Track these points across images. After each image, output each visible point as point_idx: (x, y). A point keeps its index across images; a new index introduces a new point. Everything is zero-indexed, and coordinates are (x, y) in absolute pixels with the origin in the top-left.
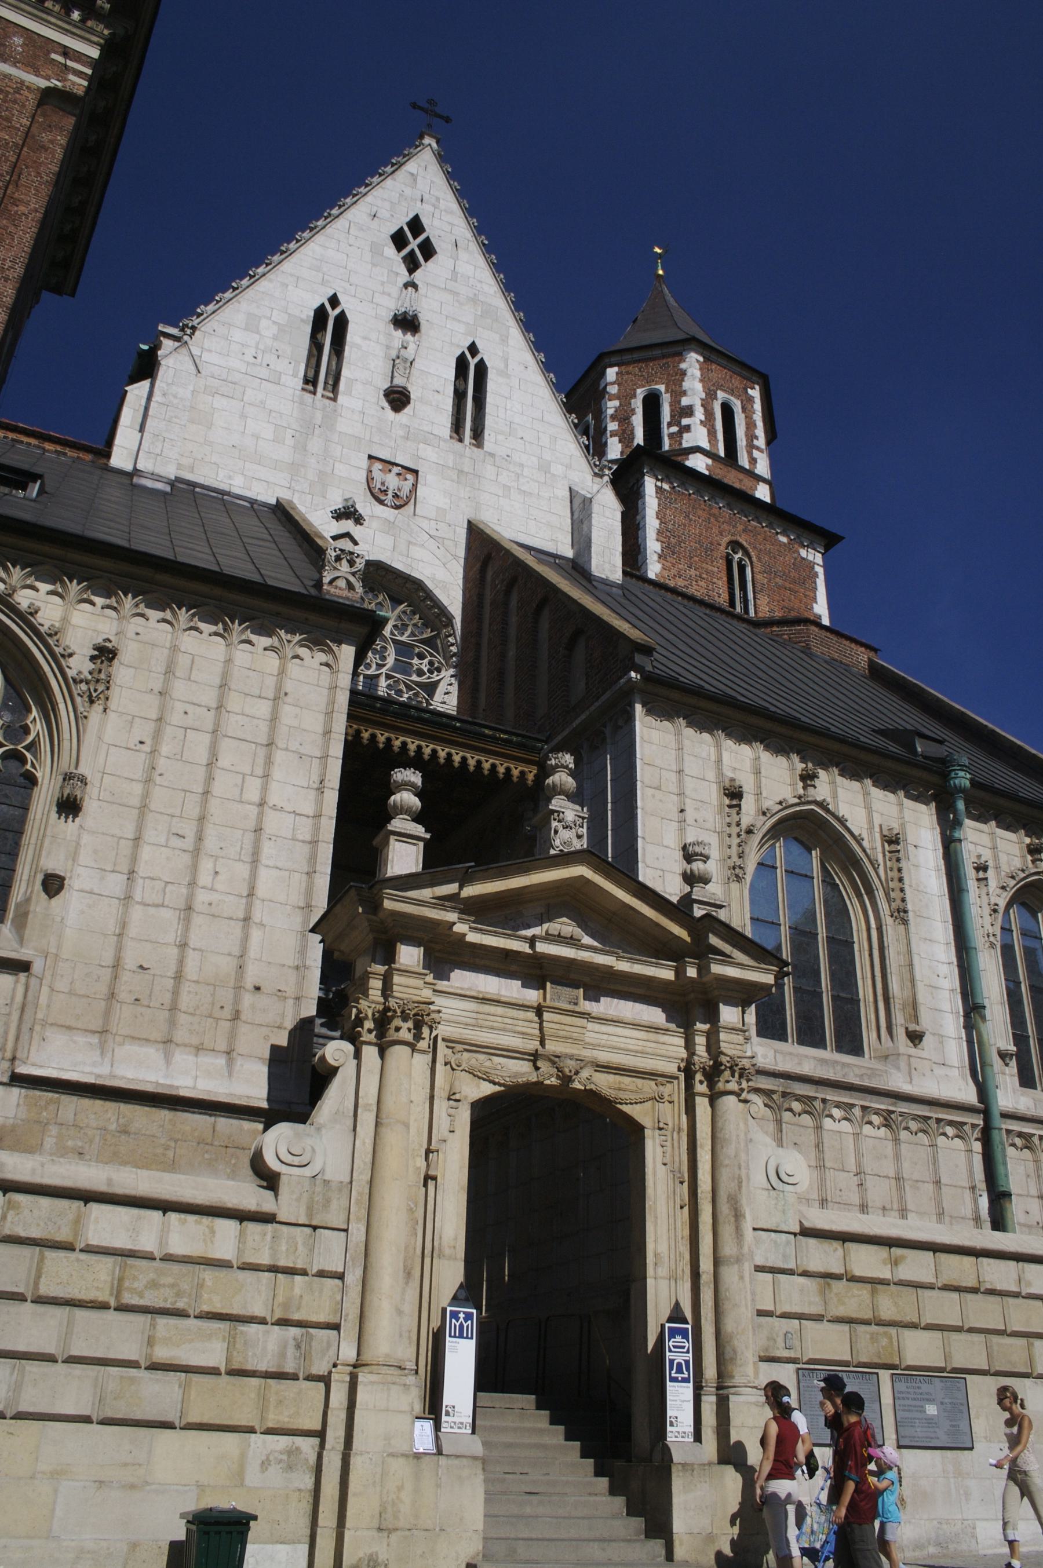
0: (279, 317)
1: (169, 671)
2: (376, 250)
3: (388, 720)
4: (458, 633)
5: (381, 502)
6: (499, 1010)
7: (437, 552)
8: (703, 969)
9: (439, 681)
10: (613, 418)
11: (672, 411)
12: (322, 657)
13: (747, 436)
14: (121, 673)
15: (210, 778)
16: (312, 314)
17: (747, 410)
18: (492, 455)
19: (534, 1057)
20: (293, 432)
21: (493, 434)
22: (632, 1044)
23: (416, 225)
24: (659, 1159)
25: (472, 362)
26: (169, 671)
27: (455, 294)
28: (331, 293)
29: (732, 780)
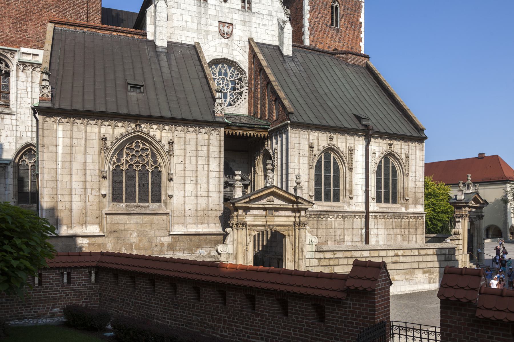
1: (185, 144)
3: (232, 128)
4: (248, 77)
5: (223, 37)
6: (258, 218)
7: (240, 51)
8: (297, 206)
9: (243, 91)
12: (217, 133)
14: (175, 146)
15: (197, 167)
18: (254, 13)
19: (265, 226)
20: (196, 17)
21: (254, 4)
22: (284, 220)
26: (185, 144)
29: (312, 143)
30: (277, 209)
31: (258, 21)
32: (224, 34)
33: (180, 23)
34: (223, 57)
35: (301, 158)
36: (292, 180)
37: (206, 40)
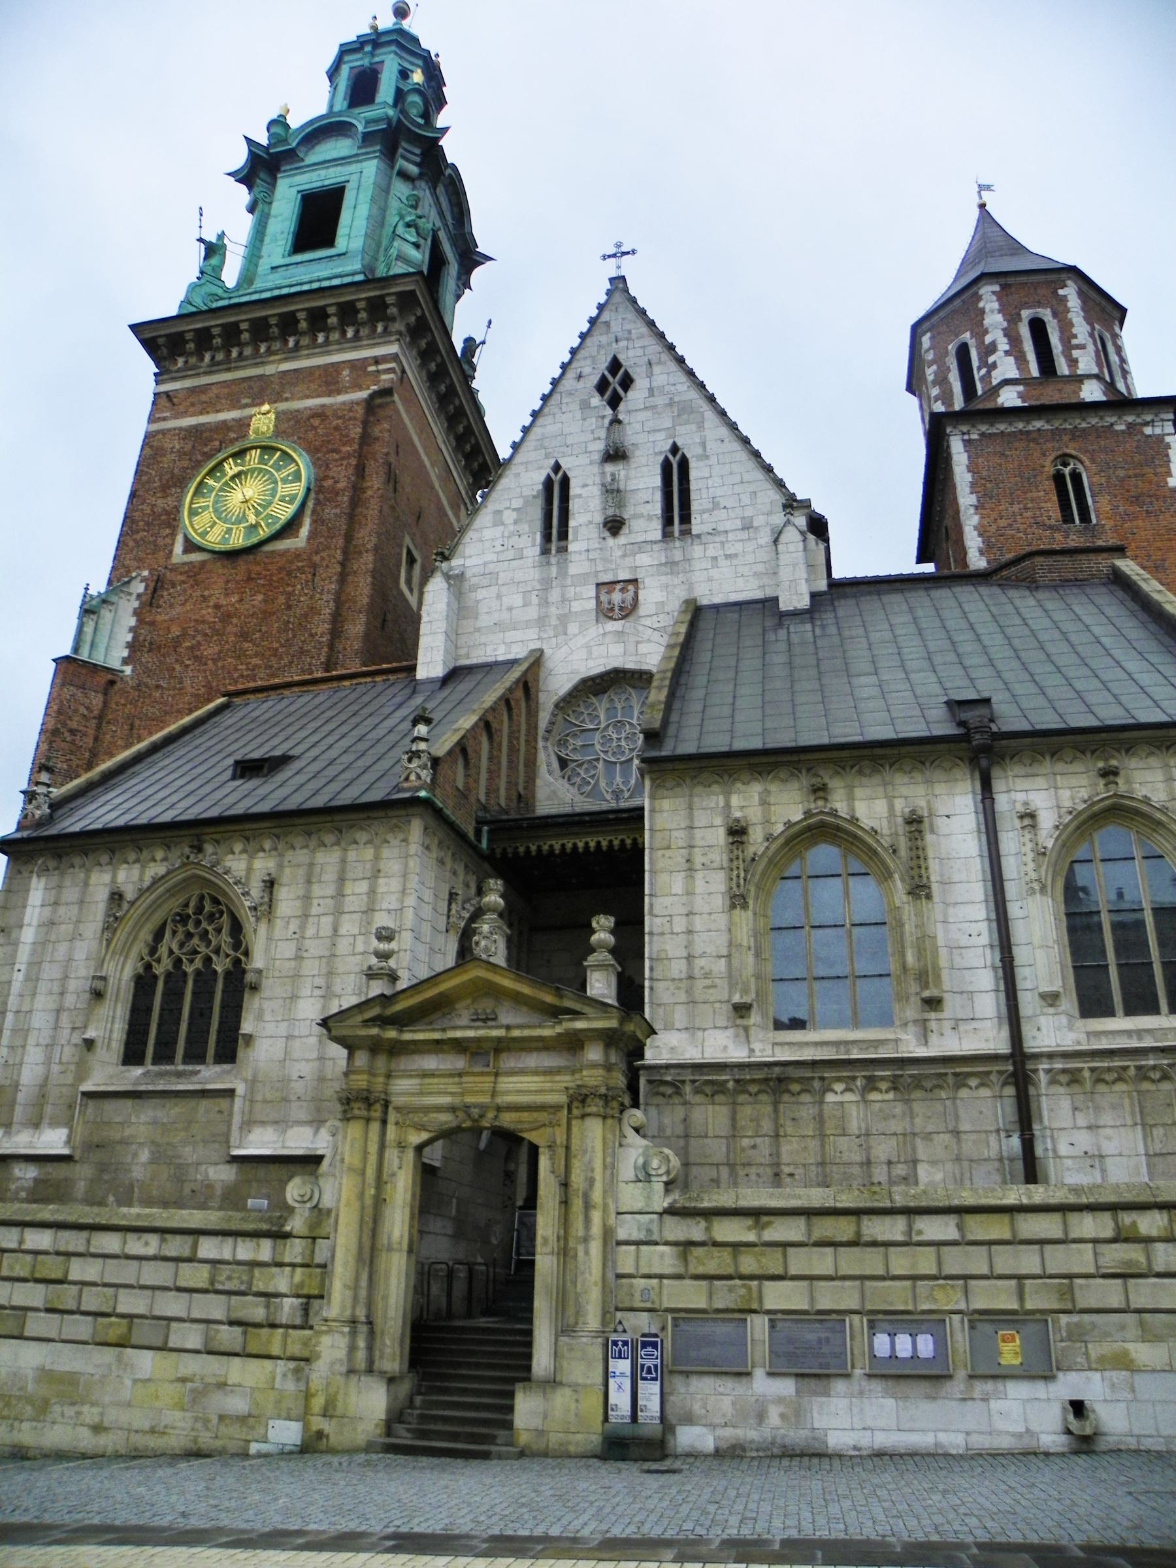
0: (518, 503)
1: (309, 882)
2: (585, 405)
5: (611, 618)
6: (436, 1080)
10: (934, 383)
11: (979, 354)
12: (401, 836)
13: (1061, 339)
16: (540, 487)
17: (1061, 312)
18: (699, 536)
22: (533, 1087)
23: (615, 365)
24: (549, 1168)
25: (675, 462)
26: (309, 882)
27: (653, 408)
28: (552, 462)
29: (737, 820)
30: (501, 1047)
31: (711, 552)
32: (612, 609)
33: (496, 617)
34: (609, 667)
35: (699, 875)
36: (663, 955)
37: (561, 638)
